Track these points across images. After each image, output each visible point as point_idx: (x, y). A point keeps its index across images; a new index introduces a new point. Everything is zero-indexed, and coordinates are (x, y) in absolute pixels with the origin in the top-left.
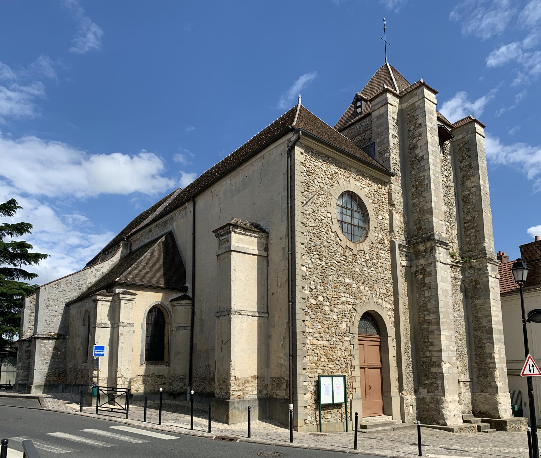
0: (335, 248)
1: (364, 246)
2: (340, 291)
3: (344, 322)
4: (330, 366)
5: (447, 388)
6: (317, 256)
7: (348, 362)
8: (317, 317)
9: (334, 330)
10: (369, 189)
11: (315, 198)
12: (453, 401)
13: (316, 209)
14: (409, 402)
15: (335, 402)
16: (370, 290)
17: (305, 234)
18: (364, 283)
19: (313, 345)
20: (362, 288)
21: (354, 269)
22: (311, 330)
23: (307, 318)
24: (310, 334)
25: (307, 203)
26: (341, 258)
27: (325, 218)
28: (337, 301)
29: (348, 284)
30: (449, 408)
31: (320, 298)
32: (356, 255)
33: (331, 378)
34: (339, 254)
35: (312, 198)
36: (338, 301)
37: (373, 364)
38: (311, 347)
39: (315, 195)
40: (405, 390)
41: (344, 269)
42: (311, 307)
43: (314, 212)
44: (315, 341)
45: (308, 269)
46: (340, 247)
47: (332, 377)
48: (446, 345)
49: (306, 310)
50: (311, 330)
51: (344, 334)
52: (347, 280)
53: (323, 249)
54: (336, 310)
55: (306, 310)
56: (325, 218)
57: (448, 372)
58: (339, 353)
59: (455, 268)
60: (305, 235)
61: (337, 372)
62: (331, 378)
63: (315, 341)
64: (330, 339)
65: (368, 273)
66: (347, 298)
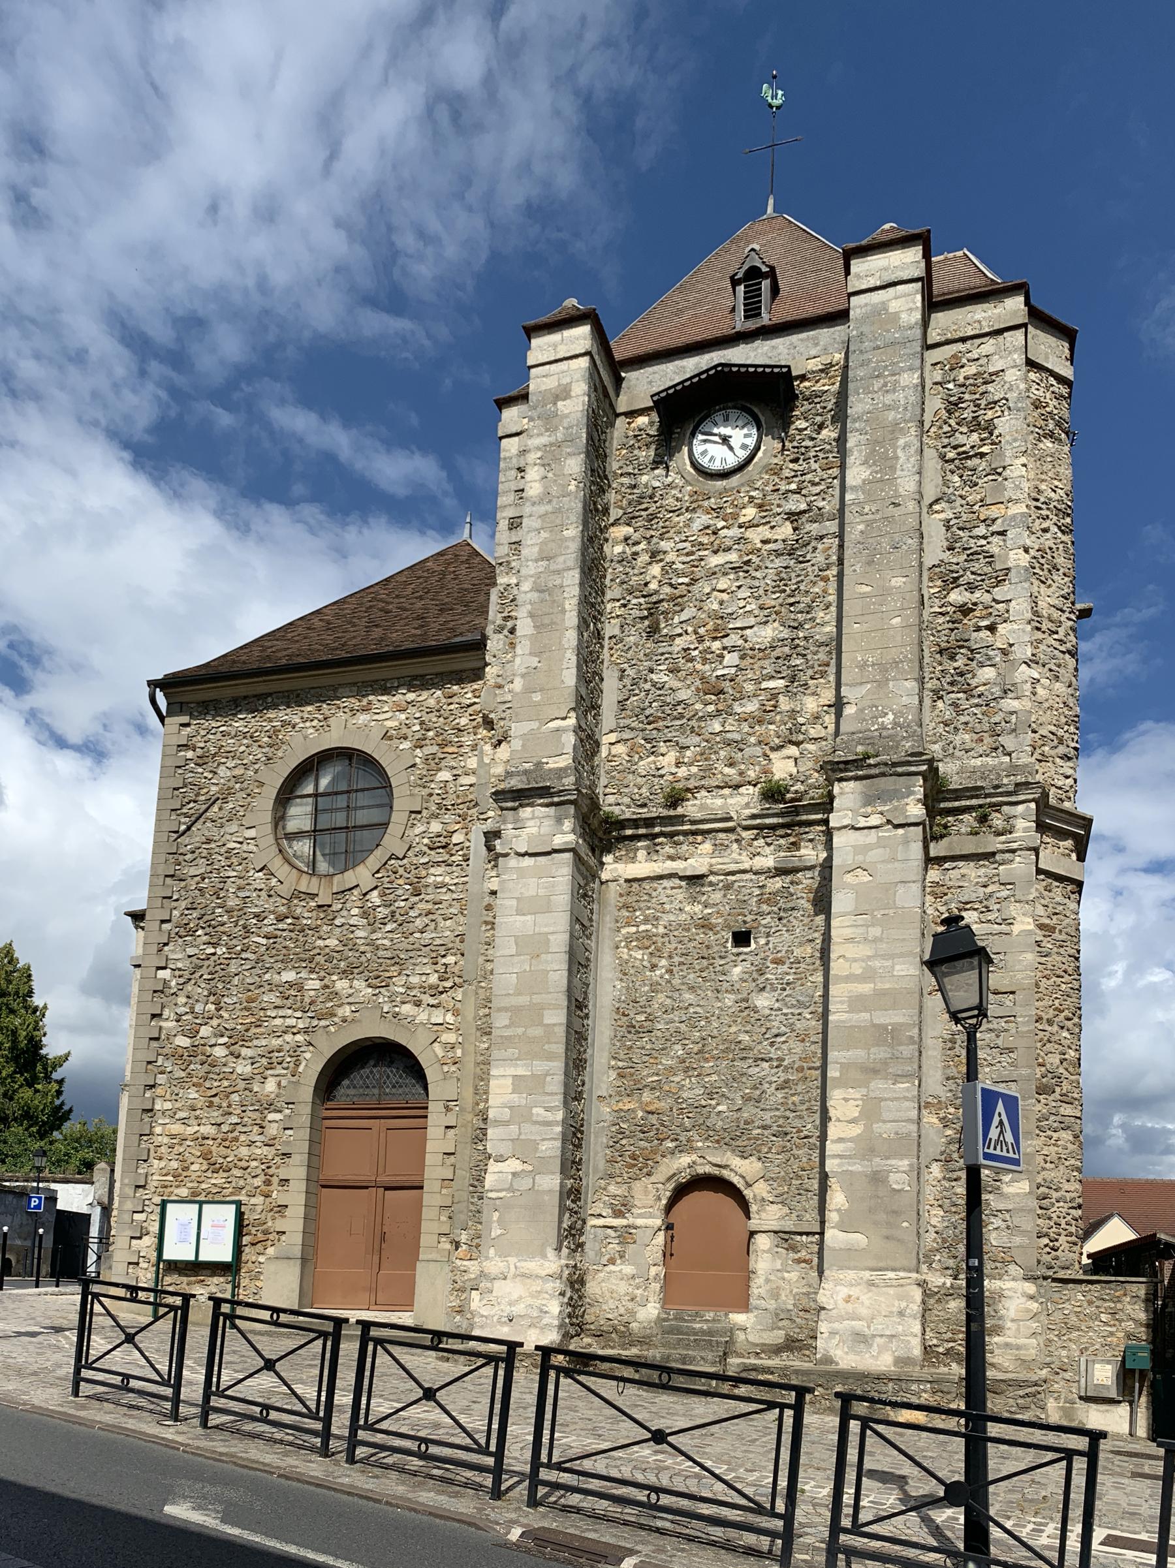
0: (263, 903)
1: (362, 875)
2: (264, 1005)
3: (270, 1079)
4: (213, 1181)
5: (493, 1235)
6: (205, 938)
7: (271, 1171)
8: (190, 1075)
9: (237, 1099)
10: (403, 716)
11: (215, 808)
12: (515, 1276)
13: (214, 833)
14: (470, 1280)
15: (201, 1258)
16: (369, 986)
17: (175, 897)
18: (345, 974)
19: (173, 1137)
20: (341, 985)
21: (320, 943)
22: (168, 1105)
23: (161, 1079)
24: (168, 1113)
25: (189, 828)
26: (280, 926)
27: (241, 843)
28: (253, 1030)
29: (291, 985)
30: (494, 1294)
31: (205, 1031)
32: (330, 906)
33: (197, 1206)
34: (272, 917)
35: (206, 811)
36: (258, 1030)
37: (398, 1178)
38: (166, 1140)
39: (214, 803)
40: (464, 1247)
41: (284, 951)
42: (176, 1055)
43: (209, 841)
44: (177, 1128)
45: (177, 973)
46: (278, 899)
47: (201, 1203)
48: (509, 1108)
49: (159, 1064)
50: (168, 1105)
51: (271, 1106)
52: (289, 976)
53: (225, 918)
54: (245, 1052)
55: (159, 1064)
56: (241, 843)
57: (507, 1186)
58: (244, 1151)
59: (789, 835)
60: (177, 900)
61: (232, 1194)
62: (197, 1206)
63: (177, 1128)
64: (219, 1121)
65: (371, 943)
66: (287, 1020)
